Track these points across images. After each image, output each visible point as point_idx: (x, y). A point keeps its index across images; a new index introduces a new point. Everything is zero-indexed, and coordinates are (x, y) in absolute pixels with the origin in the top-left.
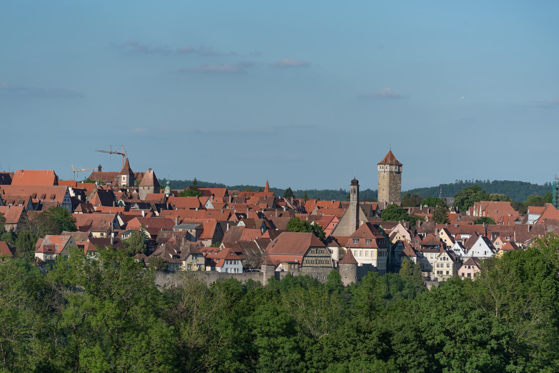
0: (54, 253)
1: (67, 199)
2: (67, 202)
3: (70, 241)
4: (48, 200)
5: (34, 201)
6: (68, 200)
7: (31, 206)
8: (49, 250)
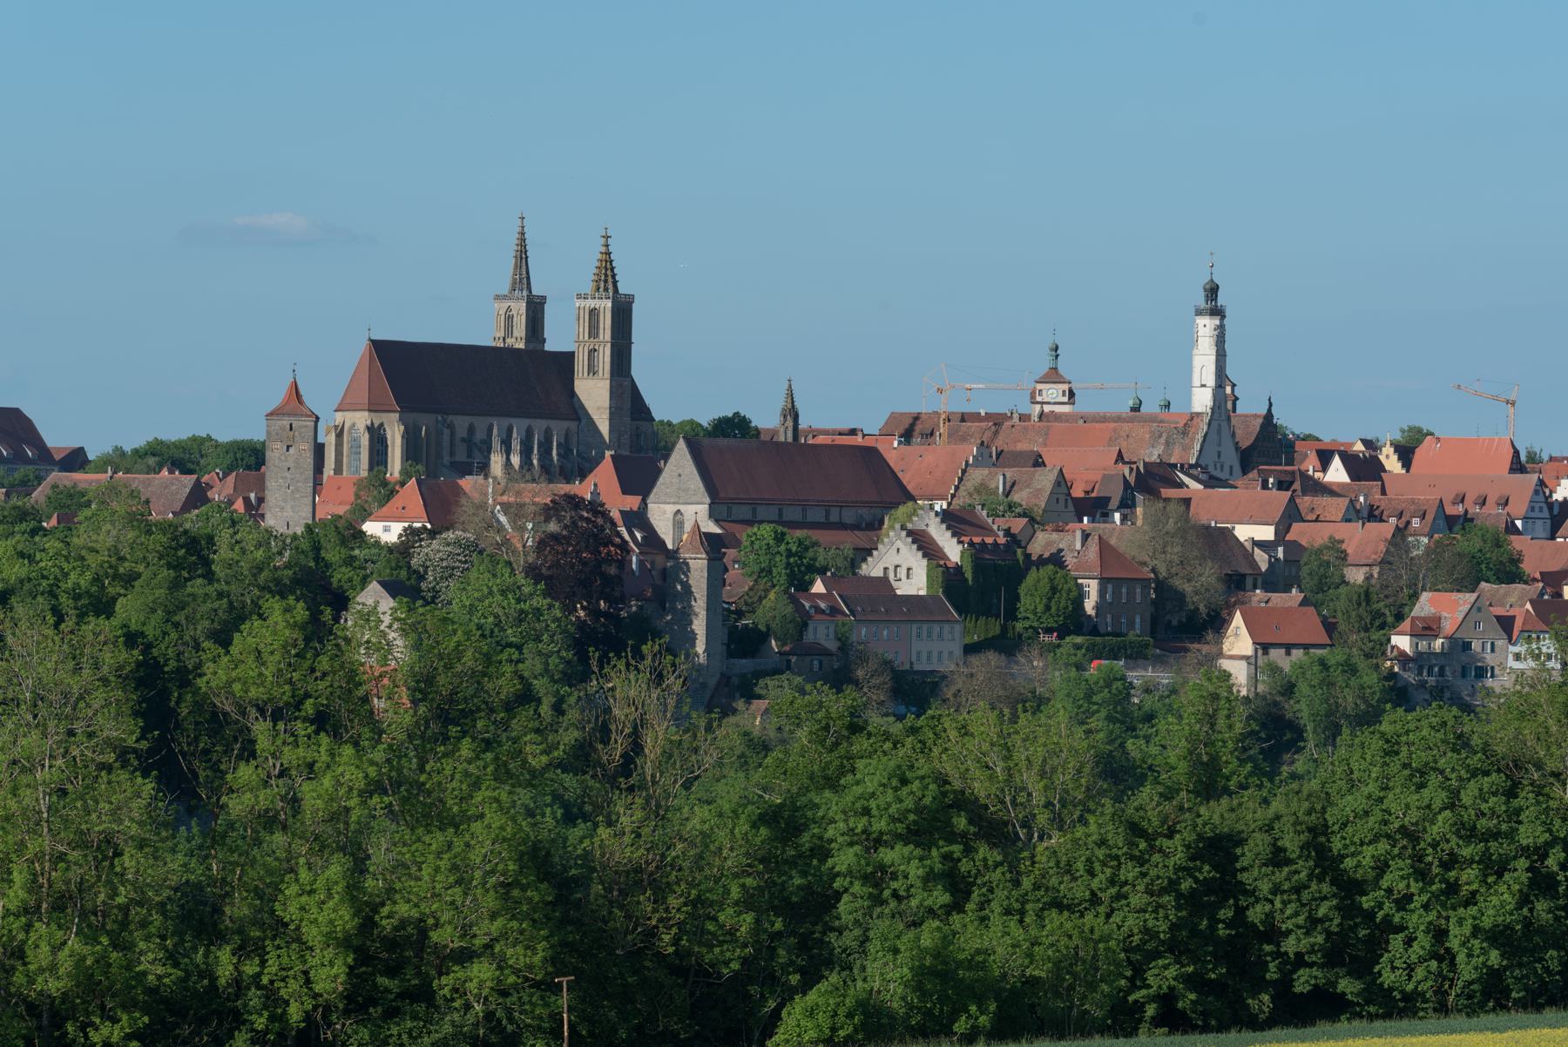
0: (1436, 636)
1: (1537, 506)
2: (1537, 514)
3: (1476, 607)
4: (1492, 509)
5: (1452, 510)
6: (1541, 510)
7: (1442, 523)
8: (1427, 629)
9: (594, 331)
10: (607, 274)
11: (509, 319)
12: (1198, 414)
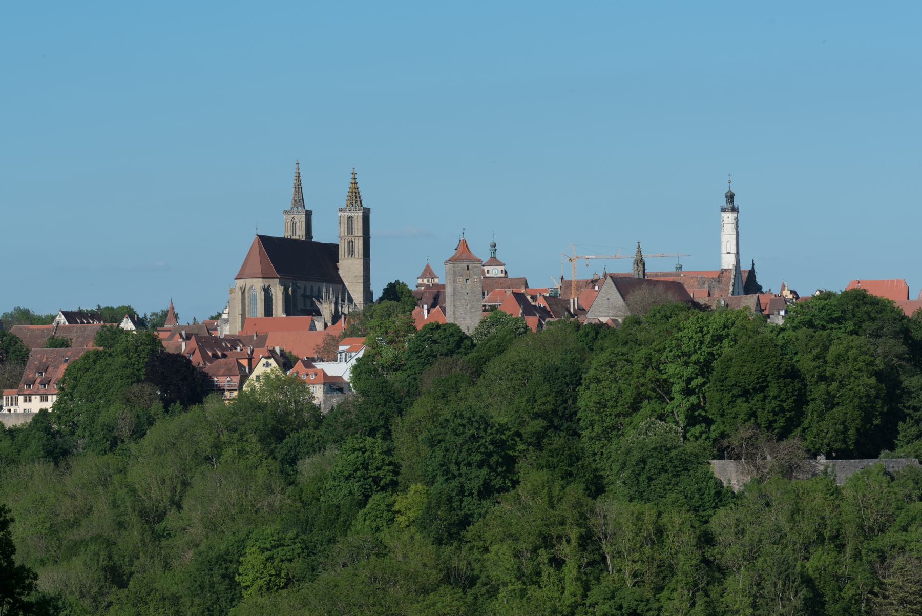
9: (351, 230)
10: (355, 196)
11: (294, 224)
12: (726, 270)
